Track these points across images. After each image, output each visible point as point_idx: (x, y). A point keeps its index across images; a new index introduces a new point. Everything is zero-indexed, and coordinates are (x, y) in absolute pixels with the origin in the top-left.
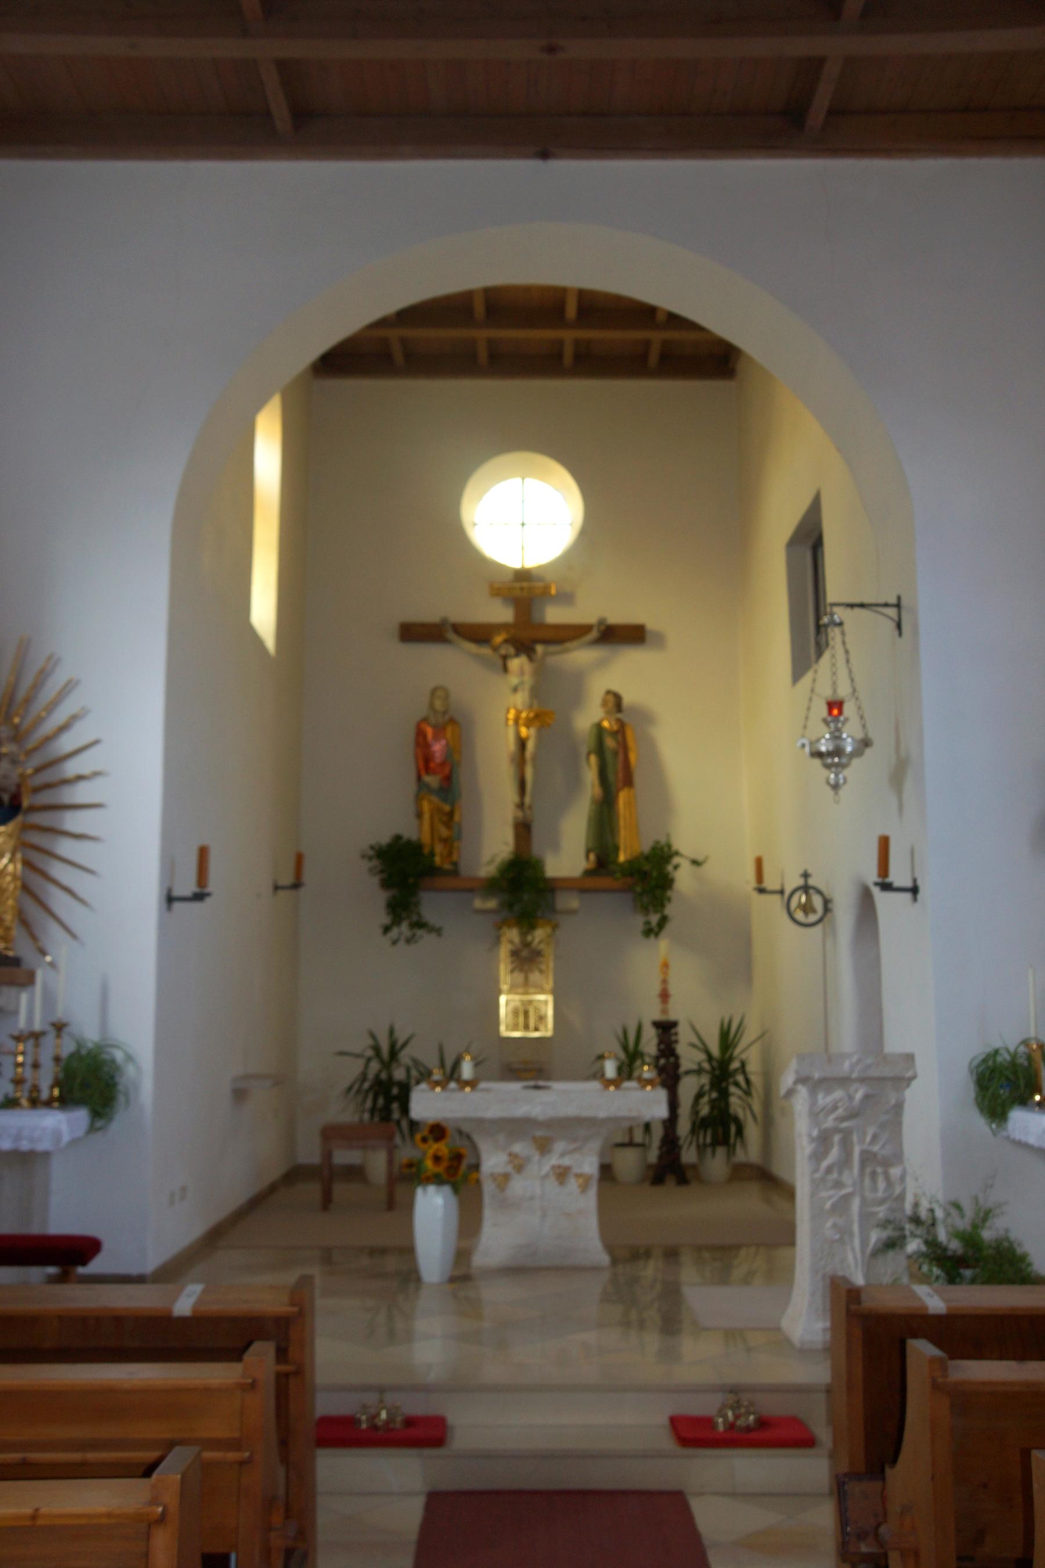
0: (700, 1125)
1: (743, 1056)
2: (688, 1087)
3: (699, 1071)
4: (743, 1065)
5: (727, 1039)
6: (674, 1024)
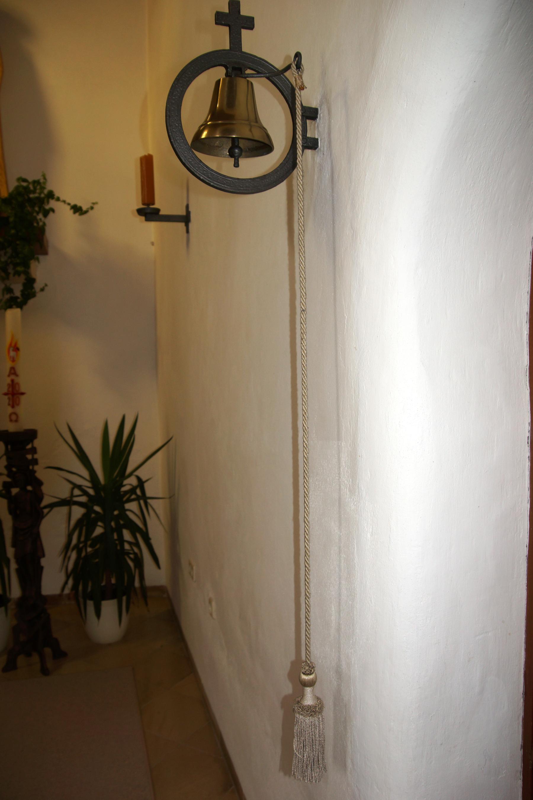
0: (81, 573)
1: (142, 473)
2: (54, 530)
3: (67, 502)
4: (141, 483)
5: (118, 451)
6: (32, 434)
